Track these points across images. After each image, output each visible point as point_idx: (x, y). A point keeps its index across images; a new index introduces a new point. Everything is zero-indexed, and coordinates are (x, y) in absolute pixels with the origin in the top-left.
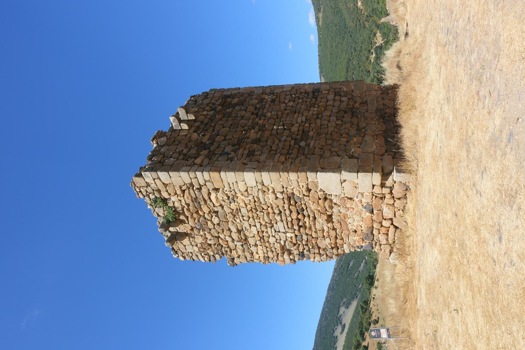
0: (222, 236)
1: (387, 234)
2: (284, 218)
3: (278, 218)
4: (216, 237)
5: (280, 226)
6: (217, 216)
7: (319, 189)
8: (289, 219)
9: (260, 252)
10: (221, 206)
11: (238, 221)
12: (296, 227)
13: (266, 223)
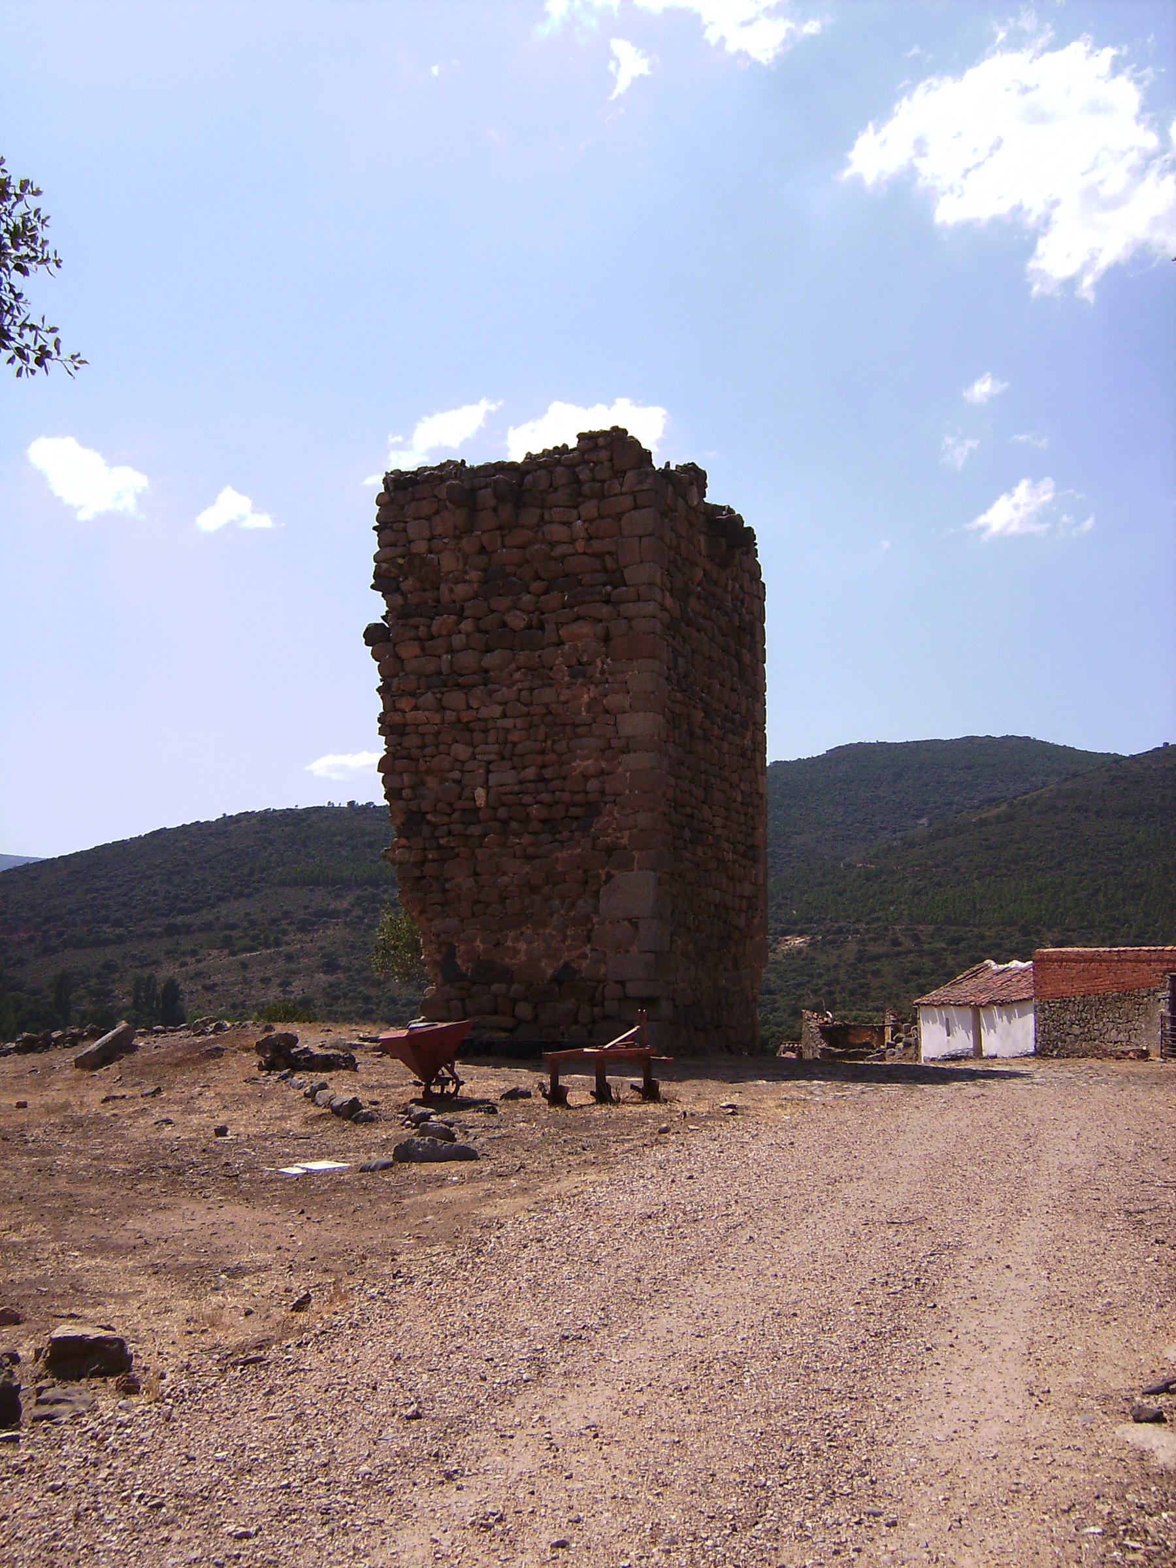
0: (466, 626)
1: (495, 1013)
2: (531, 786)
3: (530, 773)
4: (462, 609)
5: (503, 777)
6: (529, 627)
7: (613, 872)
8: (527, 799)
9: (421, 715)
10: (561, 643)
11: (517, 675)
12: (502, 812)
13: (515, 744)
